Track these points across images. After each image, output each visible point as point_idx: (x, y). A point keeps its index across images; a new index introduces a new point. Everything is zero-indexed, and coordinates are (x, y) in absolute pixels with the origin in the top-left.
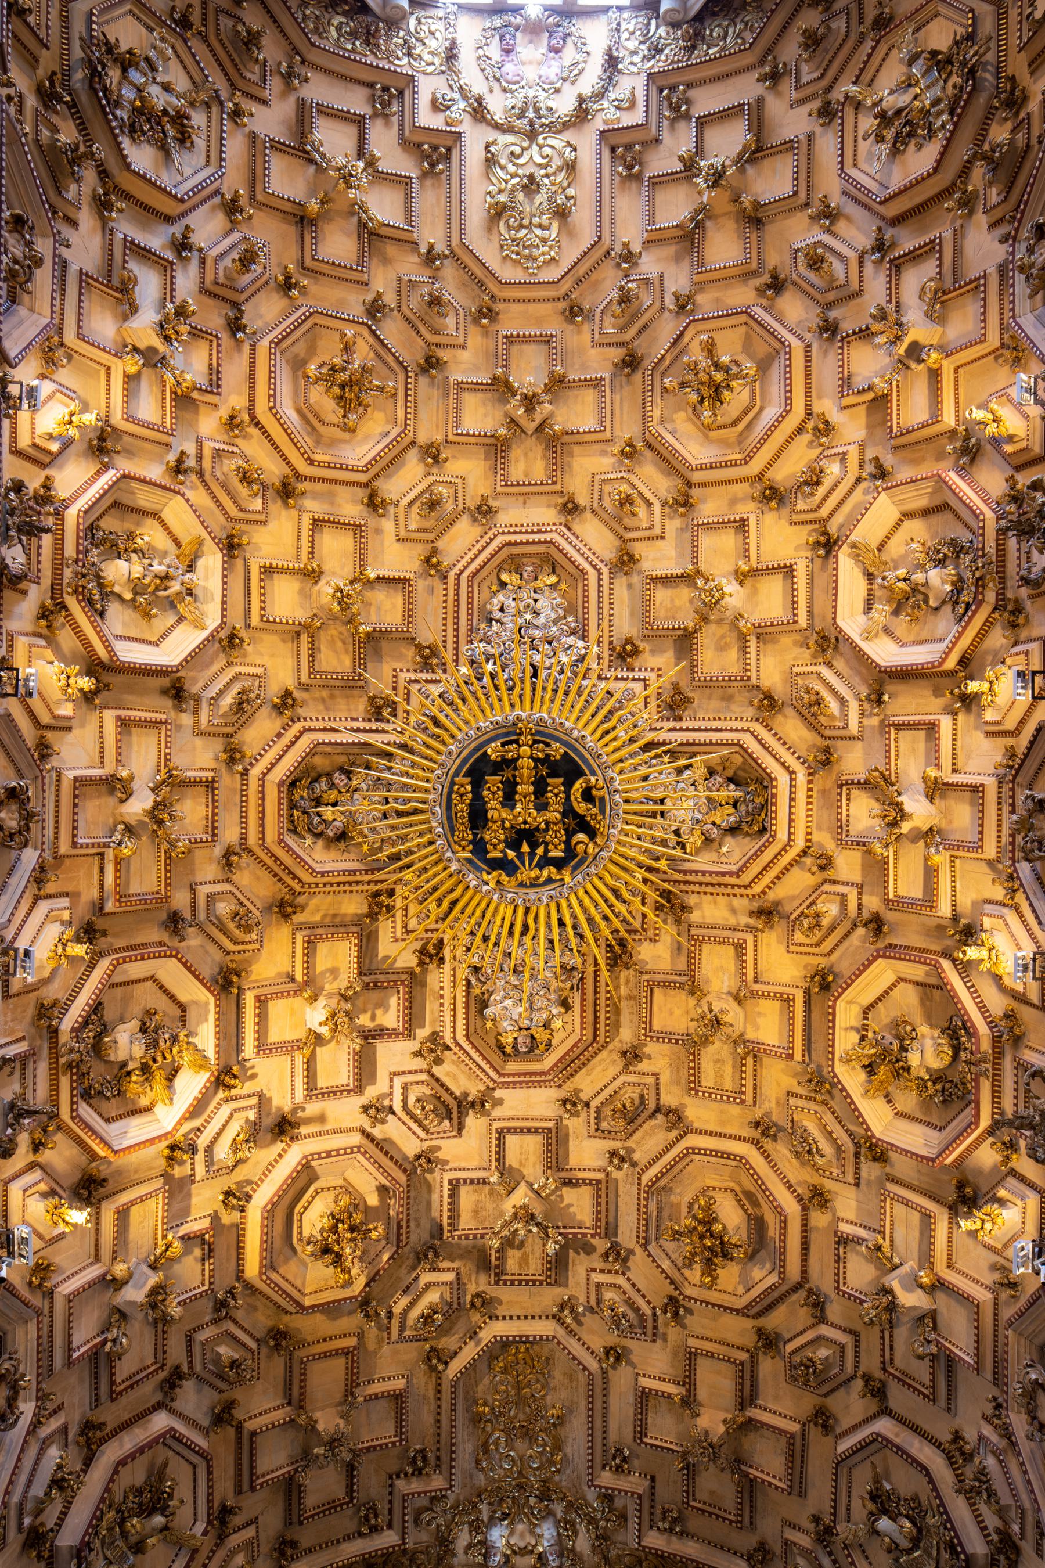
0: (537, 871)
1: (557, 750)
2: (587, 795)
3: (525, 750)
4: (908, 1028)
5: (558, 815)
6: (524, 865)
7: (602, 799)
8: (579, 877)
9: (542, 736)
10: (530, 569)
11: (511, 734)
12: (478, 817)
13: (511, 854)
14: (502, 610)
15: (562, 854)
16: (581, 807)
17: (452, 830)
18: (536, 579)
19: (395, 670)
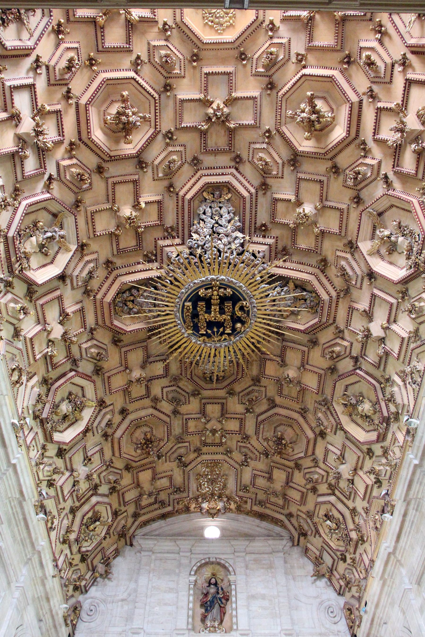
0: (220, 338)
1: (229, 293)
2: (242, 308)
3: (215, 293)
4: (361, 398)
5: (229, 317)
6: (214, 335)
7: (248, 311)
8: (238, 338)
9: (223, 286)
10: (218, 193)
11: (208, 286)
12: (195, 315)
13: (209, 332)
14: (204, 213)
15: (231, 332)
16: (239, 314)
17: (185, 322)
18: (220, 197)
19: (155, 239)
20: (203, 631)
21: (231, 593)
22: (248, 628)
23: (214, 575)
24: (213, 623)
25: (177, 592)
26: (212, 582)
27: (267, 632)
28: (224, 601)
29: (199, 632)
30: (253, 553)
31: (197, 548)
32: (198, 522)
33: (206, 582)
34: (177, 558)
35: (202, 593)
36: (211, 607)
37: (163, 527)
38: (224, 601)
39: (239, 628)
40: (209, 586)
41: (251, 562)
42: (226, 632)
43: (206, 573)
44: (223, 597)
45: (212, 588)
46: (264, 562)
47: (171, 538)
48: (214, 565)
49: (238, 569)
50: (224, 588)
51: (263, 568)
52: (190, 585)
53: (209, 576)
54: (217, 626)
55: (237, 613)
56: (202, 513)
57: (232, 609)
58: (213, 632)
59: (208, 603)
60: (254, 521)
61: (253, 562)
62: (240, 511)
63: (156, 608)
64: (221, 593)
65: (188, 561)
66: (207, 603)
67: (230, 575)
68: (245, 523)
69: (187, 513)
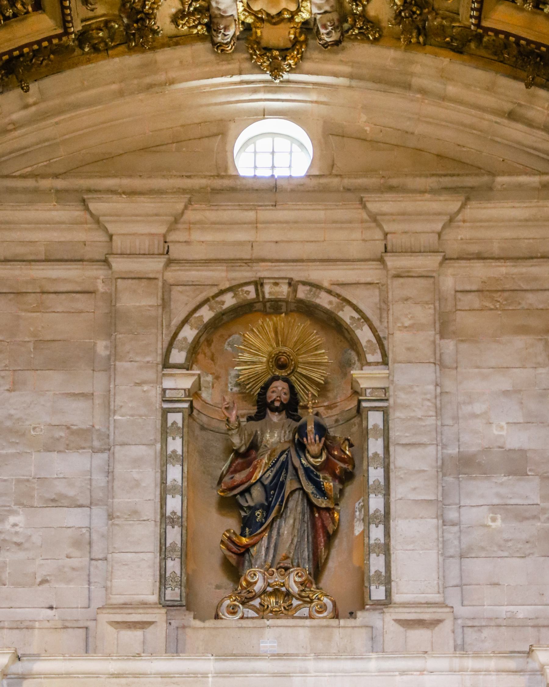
20: (233, 611)
21: (364, 448)
22: (437, 598)
23: (282, 366)
24: (277, 579)
25: (108, 449)
26: (271, 396)
27: (522, 612)
28: (329, 484)
29: (217, 617)
30: (480, 257)
31: (196, 236)
32: (200, 92)
33: (245, 395)
34: (101, 287)
35: (230, 449)
36: (267, 509)
37: (17, 125)
38: (329, 484)
39: (397, 598)
40: (260, 416)
41: (467, 300)
42: (336, 616)
43: (246, 357)
44: (326, 466)
45: (273, 427)
46: (532, 299)
47: (60, 183)
48: (281, 320)
49: (398, 335)
50: (328, 422)
51: (523, 330)
52: (165, 412)
53: (259, 368)
54: (295, 589)
55: (387, 534)
56: (215, 44)
57: (368, 520)
58: (276, 615)
59: (257, 494)
60: (490, 89)
61: (475, 301)
62: (421, 31)
63: (12, 519)
64: (314, 449)
65: (154, 301)
66: (248, 490)
67: (364, 363)
68: (444, 98)
69: (141, 48)
